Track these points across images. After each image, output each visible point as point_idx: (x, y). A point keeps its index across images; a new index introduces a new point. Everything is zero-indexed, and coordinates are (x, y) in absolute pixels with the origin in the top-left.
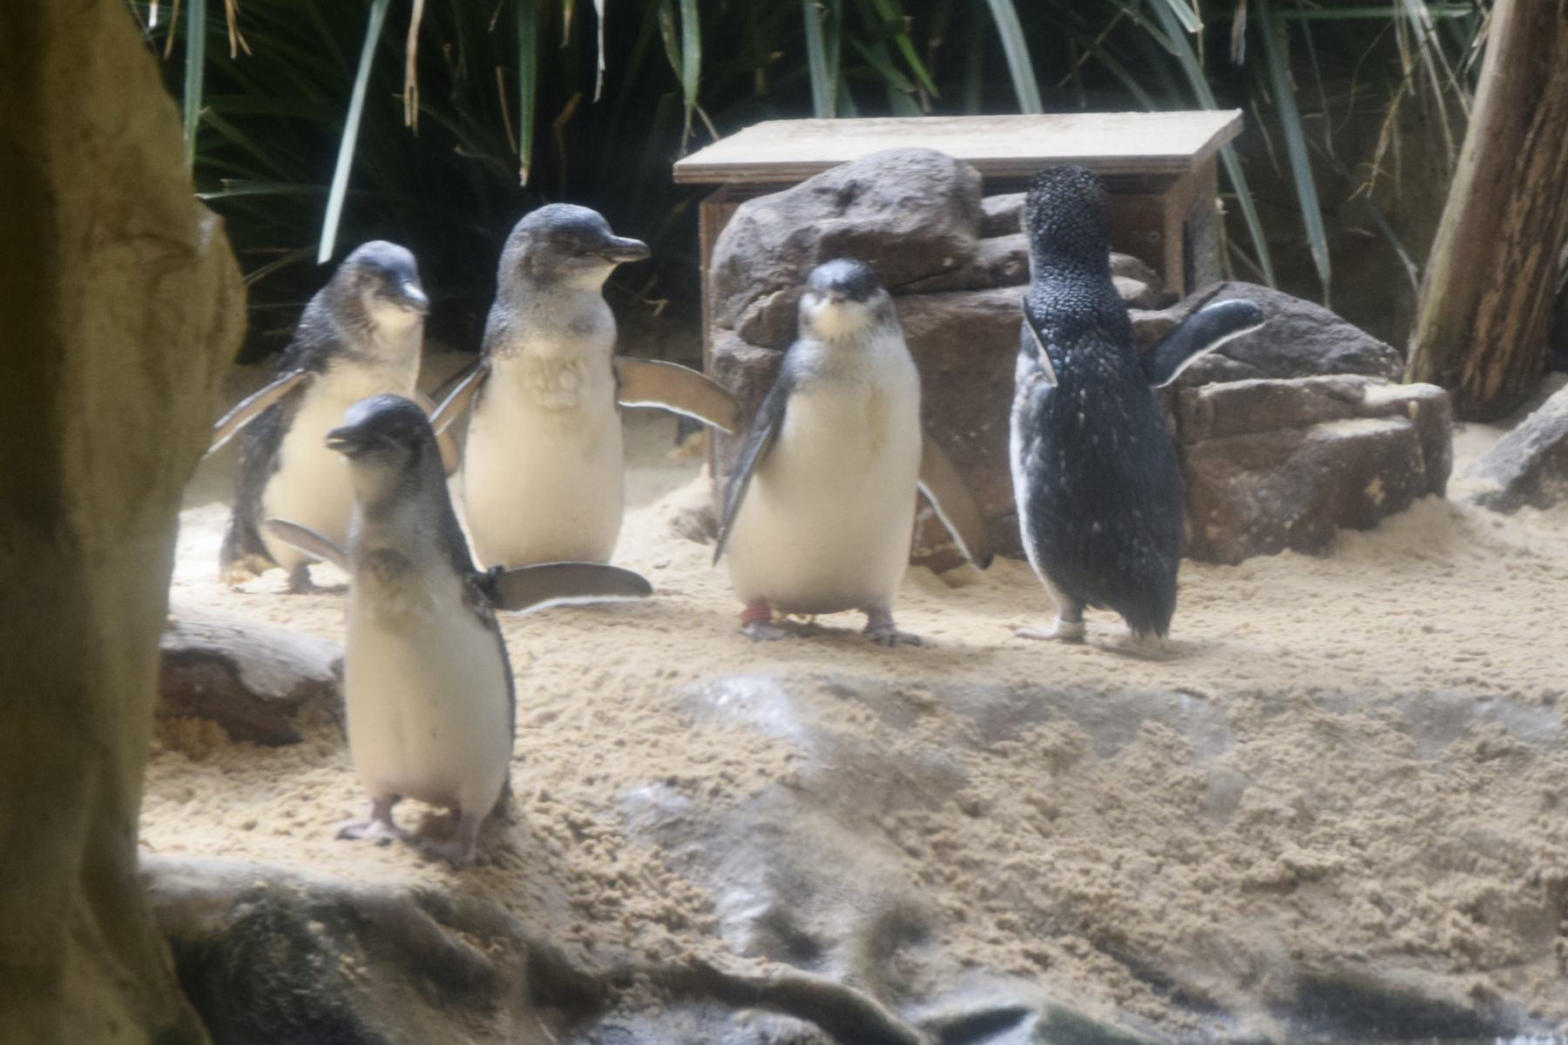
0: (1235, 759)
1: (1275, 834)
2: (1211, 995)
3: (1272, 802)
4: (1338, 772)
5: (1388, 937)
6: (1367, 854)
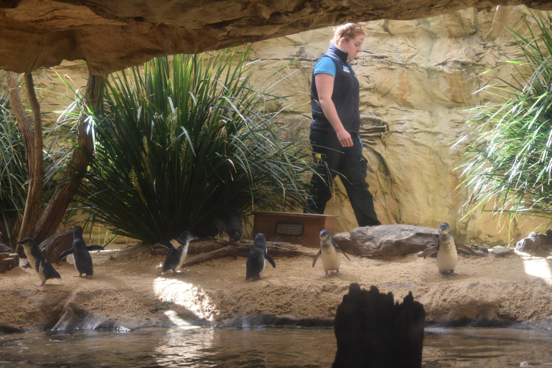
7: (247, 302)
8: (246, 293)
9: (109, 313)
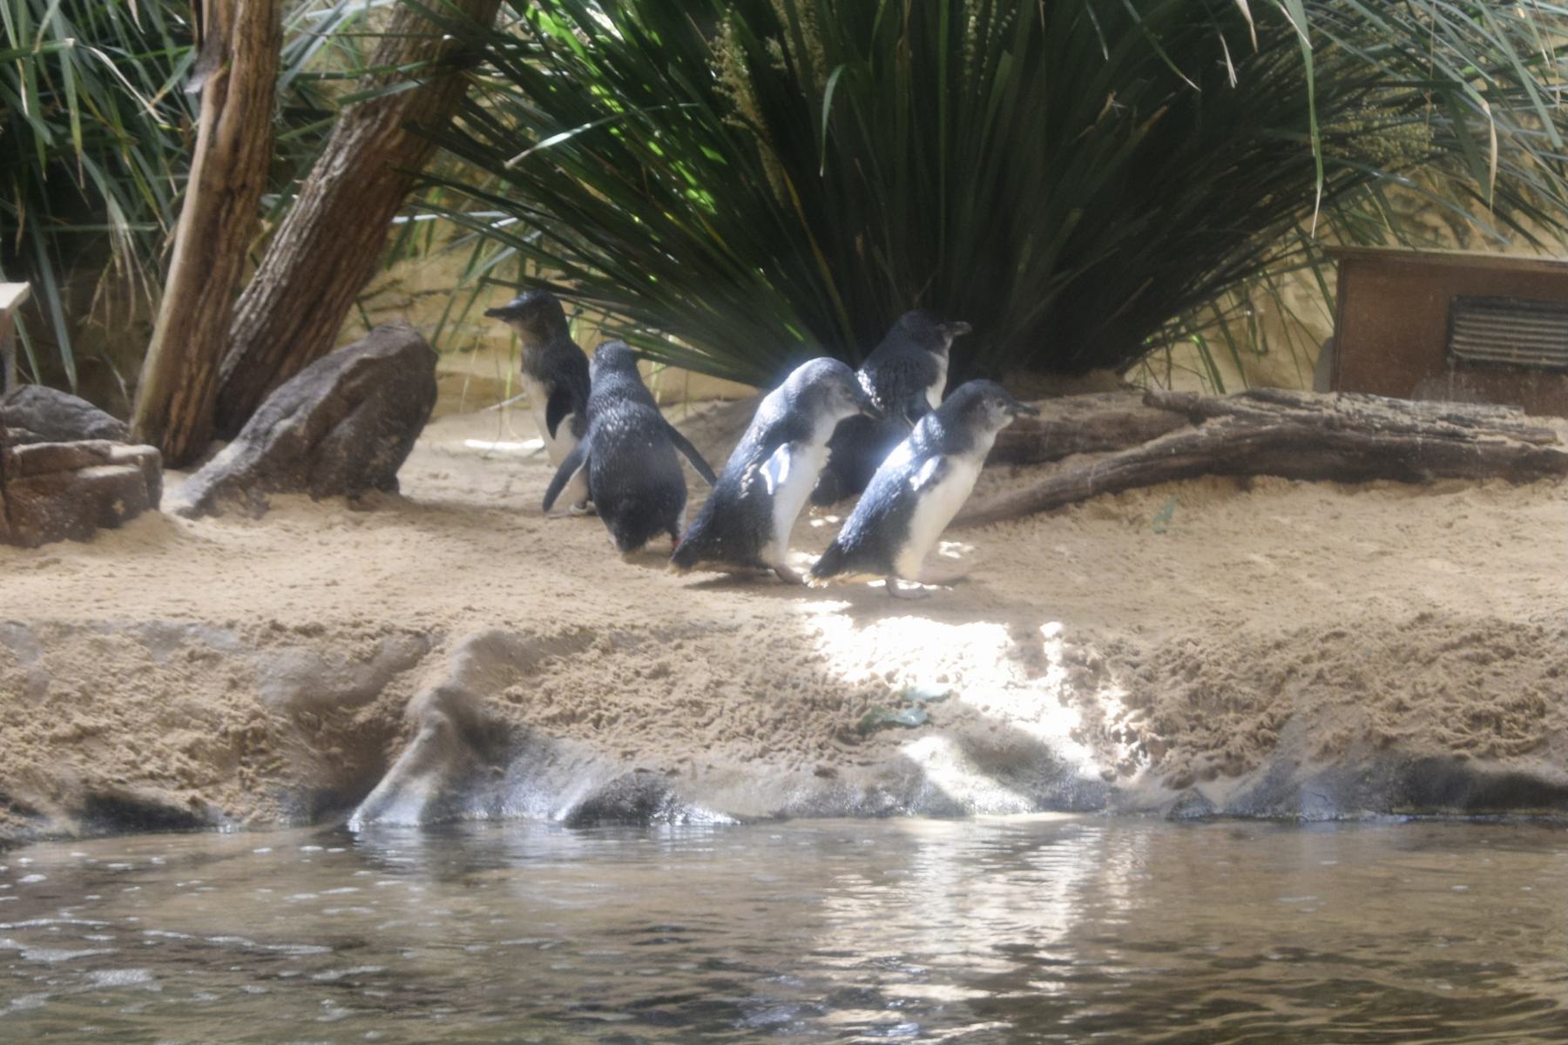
0: (44, 663)
1: (68, 708)
2: (34, 806)
3: (67, 689)
4: (106, 670)
5: (138, 768)
6: (124, 719)
7: (1323, 693)
8: (1314, 653)
9: (633, 741)
